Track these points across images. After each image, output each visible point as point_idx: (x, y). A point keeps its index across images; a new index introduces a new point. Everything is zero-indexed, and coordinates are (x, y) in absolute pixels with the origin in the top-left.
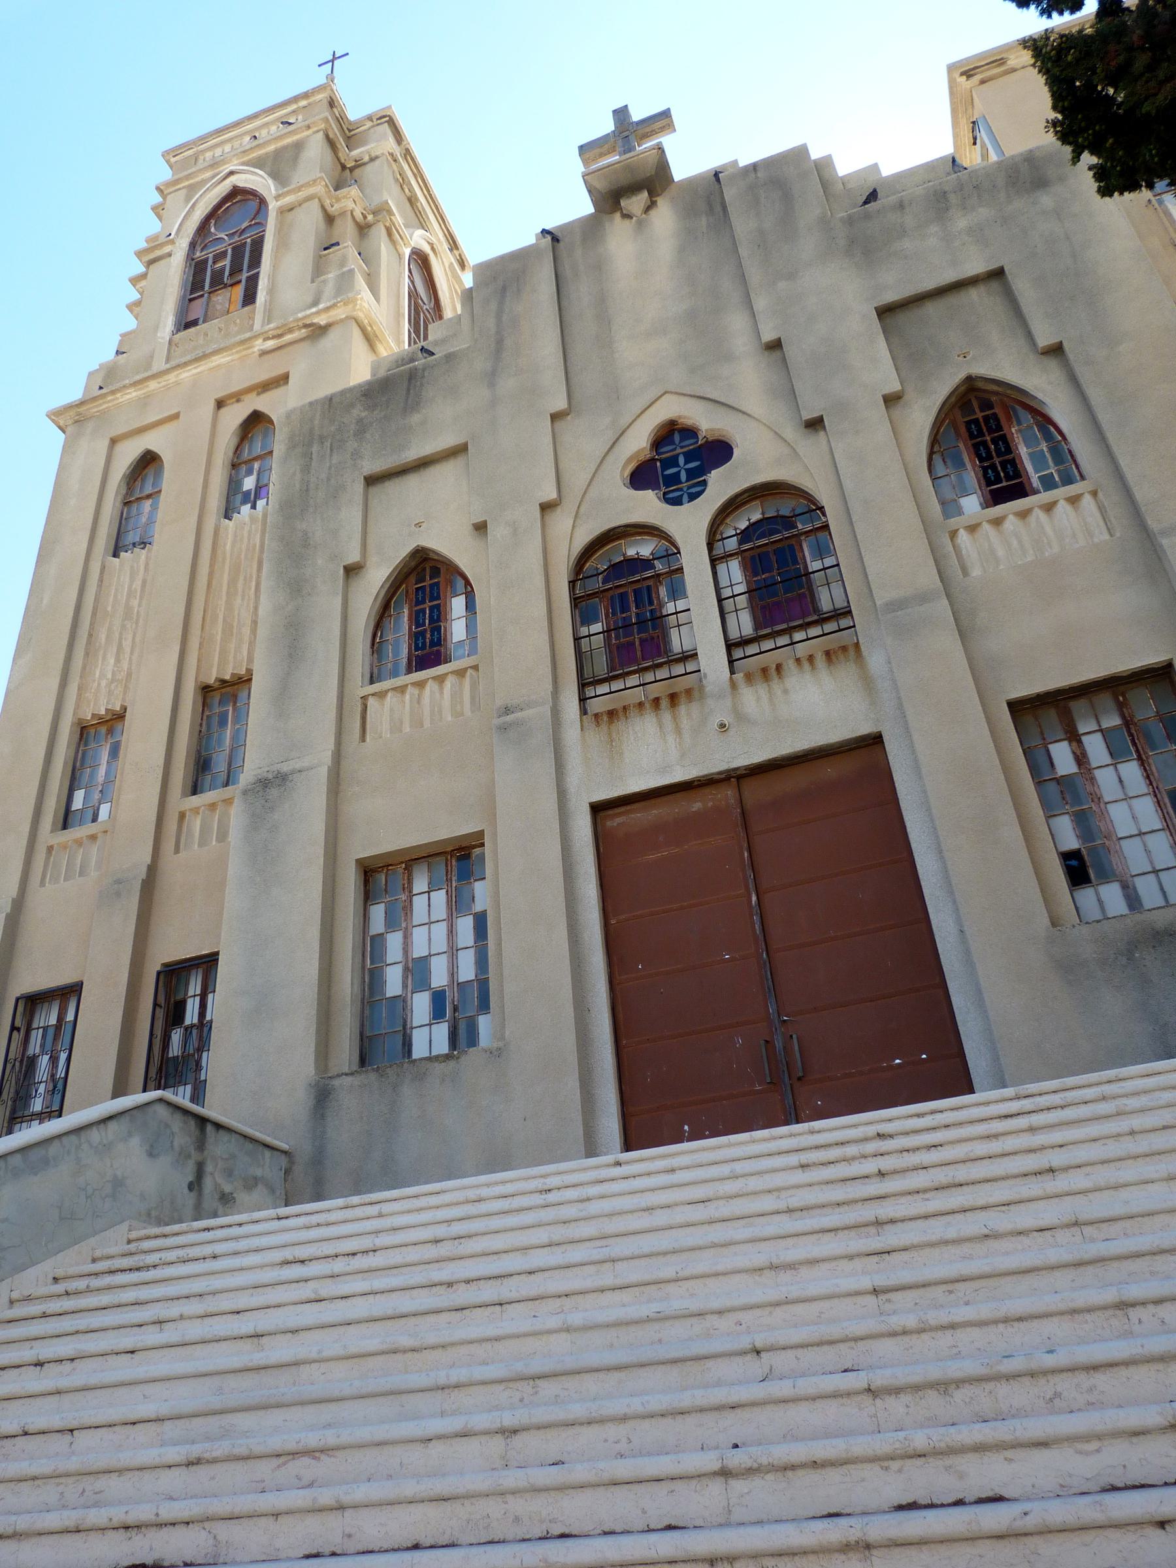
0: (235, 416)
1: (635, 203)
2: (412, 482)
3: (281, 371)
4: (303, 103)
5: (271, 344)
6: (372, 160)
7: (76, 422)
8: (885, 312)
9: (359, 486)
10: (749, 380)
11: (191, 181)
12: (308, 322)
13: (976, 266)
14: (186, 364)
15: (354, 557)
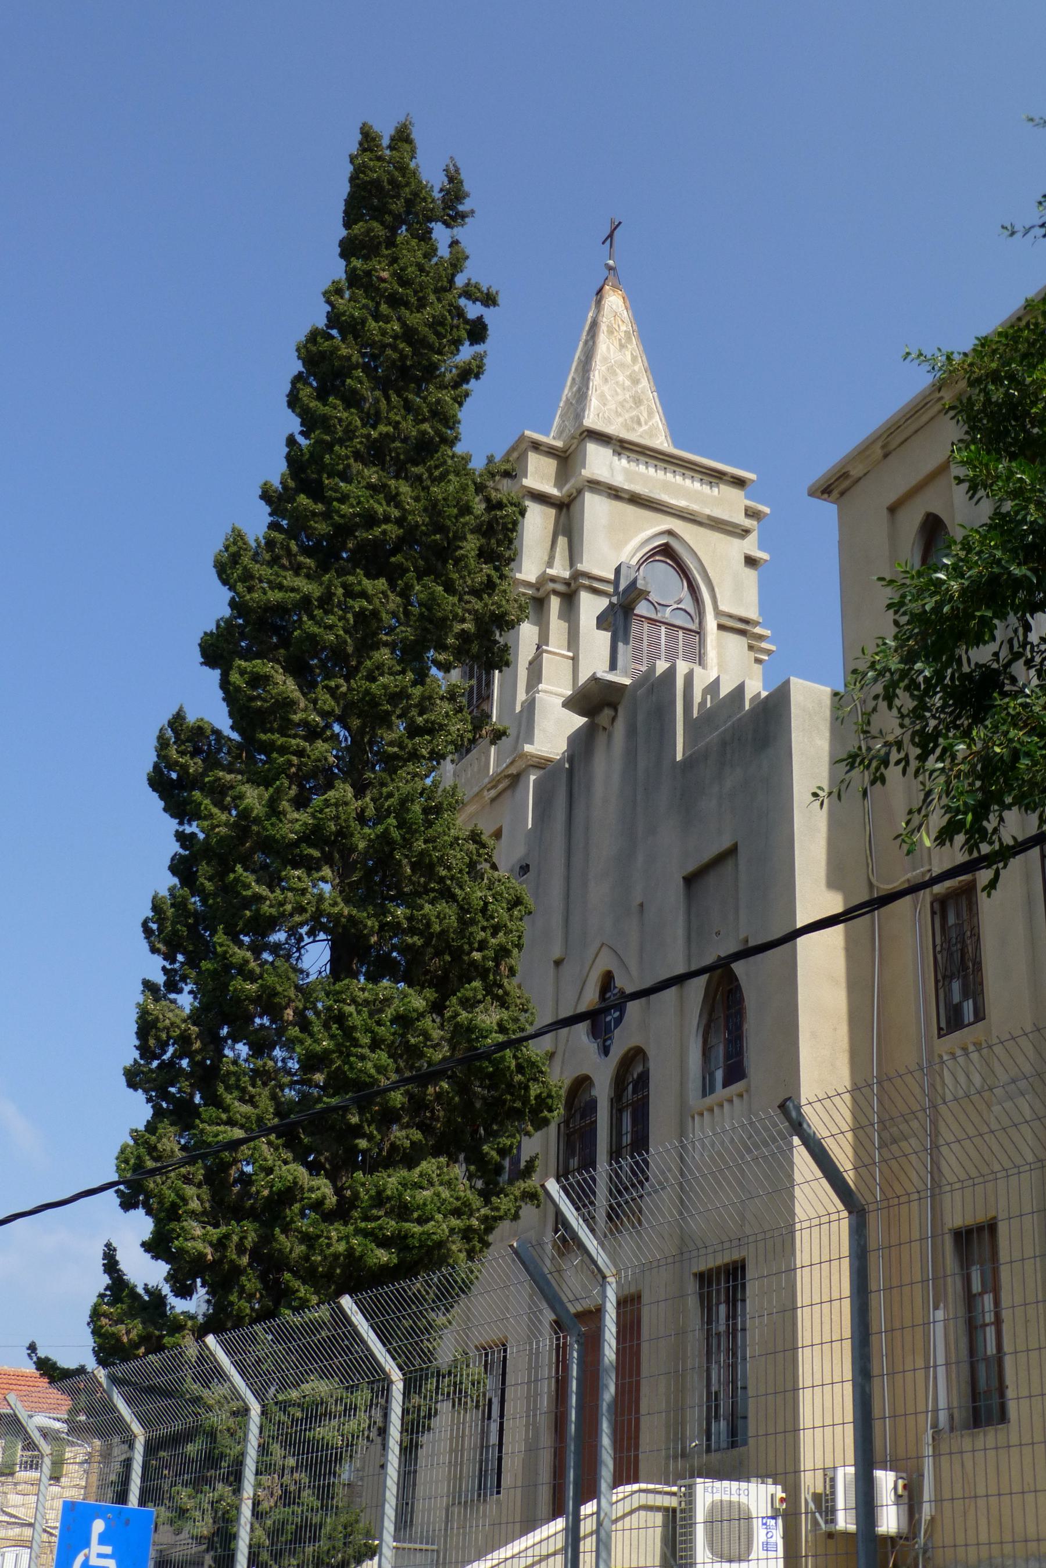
5: (493, 793)
6: (580, 492)
12: (506, 773)
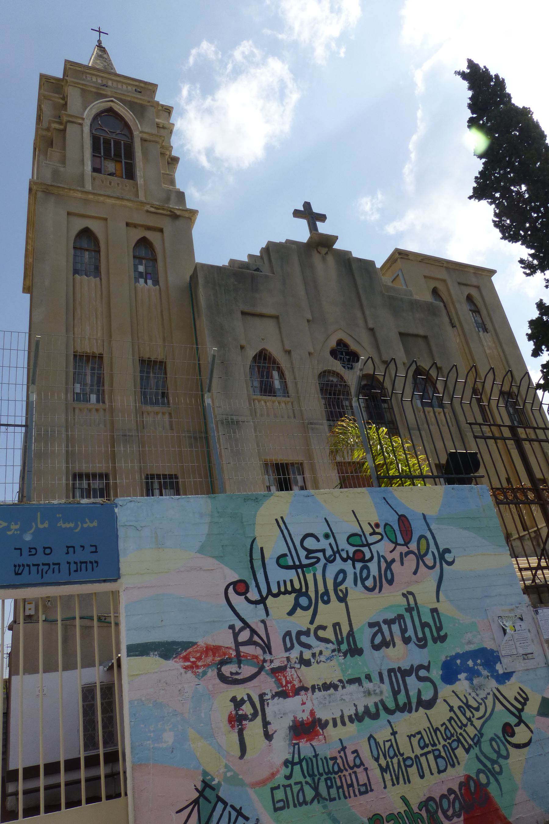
0: (137, 235)
1: (324, 250)
2: (257, 321)
3: (158, 225)
4: (142, 85)
5: (153, 210)
7: (43, 191)
8: (401, 334)
9: (239, 314)
10: (365, 338)
11: (84, 87)
12: (172, 210)
13: (421, 332)
14: (112, 197)
15: (243, 343)
